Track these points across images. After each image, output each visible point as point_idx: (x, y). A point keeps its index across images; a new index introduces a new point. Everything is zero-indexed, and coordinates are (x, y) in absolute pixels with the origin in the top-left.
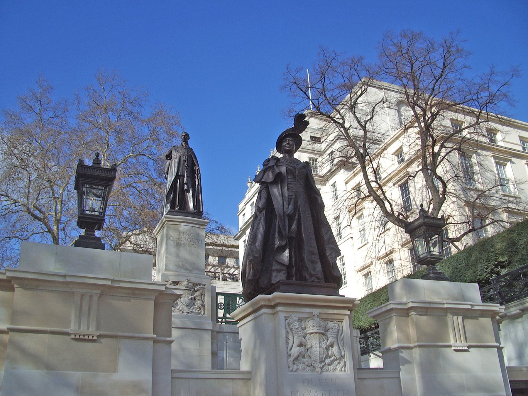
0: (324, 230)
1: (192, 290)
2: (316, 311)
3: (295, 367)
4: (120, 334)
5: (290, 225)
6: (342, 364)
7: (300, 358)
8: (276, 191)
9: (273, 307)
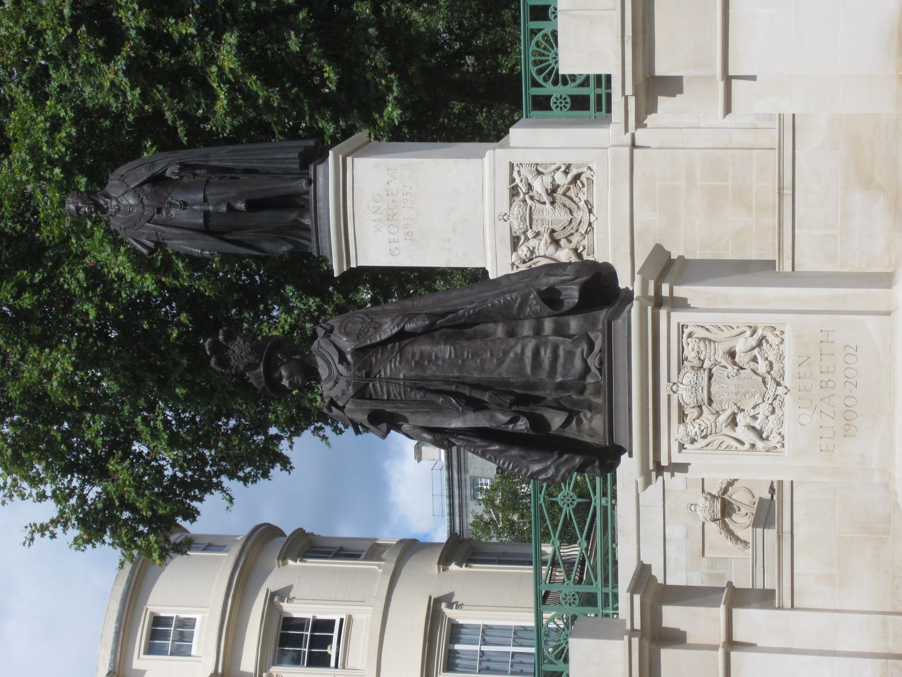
1: (529, 202)
3: (774, 440)
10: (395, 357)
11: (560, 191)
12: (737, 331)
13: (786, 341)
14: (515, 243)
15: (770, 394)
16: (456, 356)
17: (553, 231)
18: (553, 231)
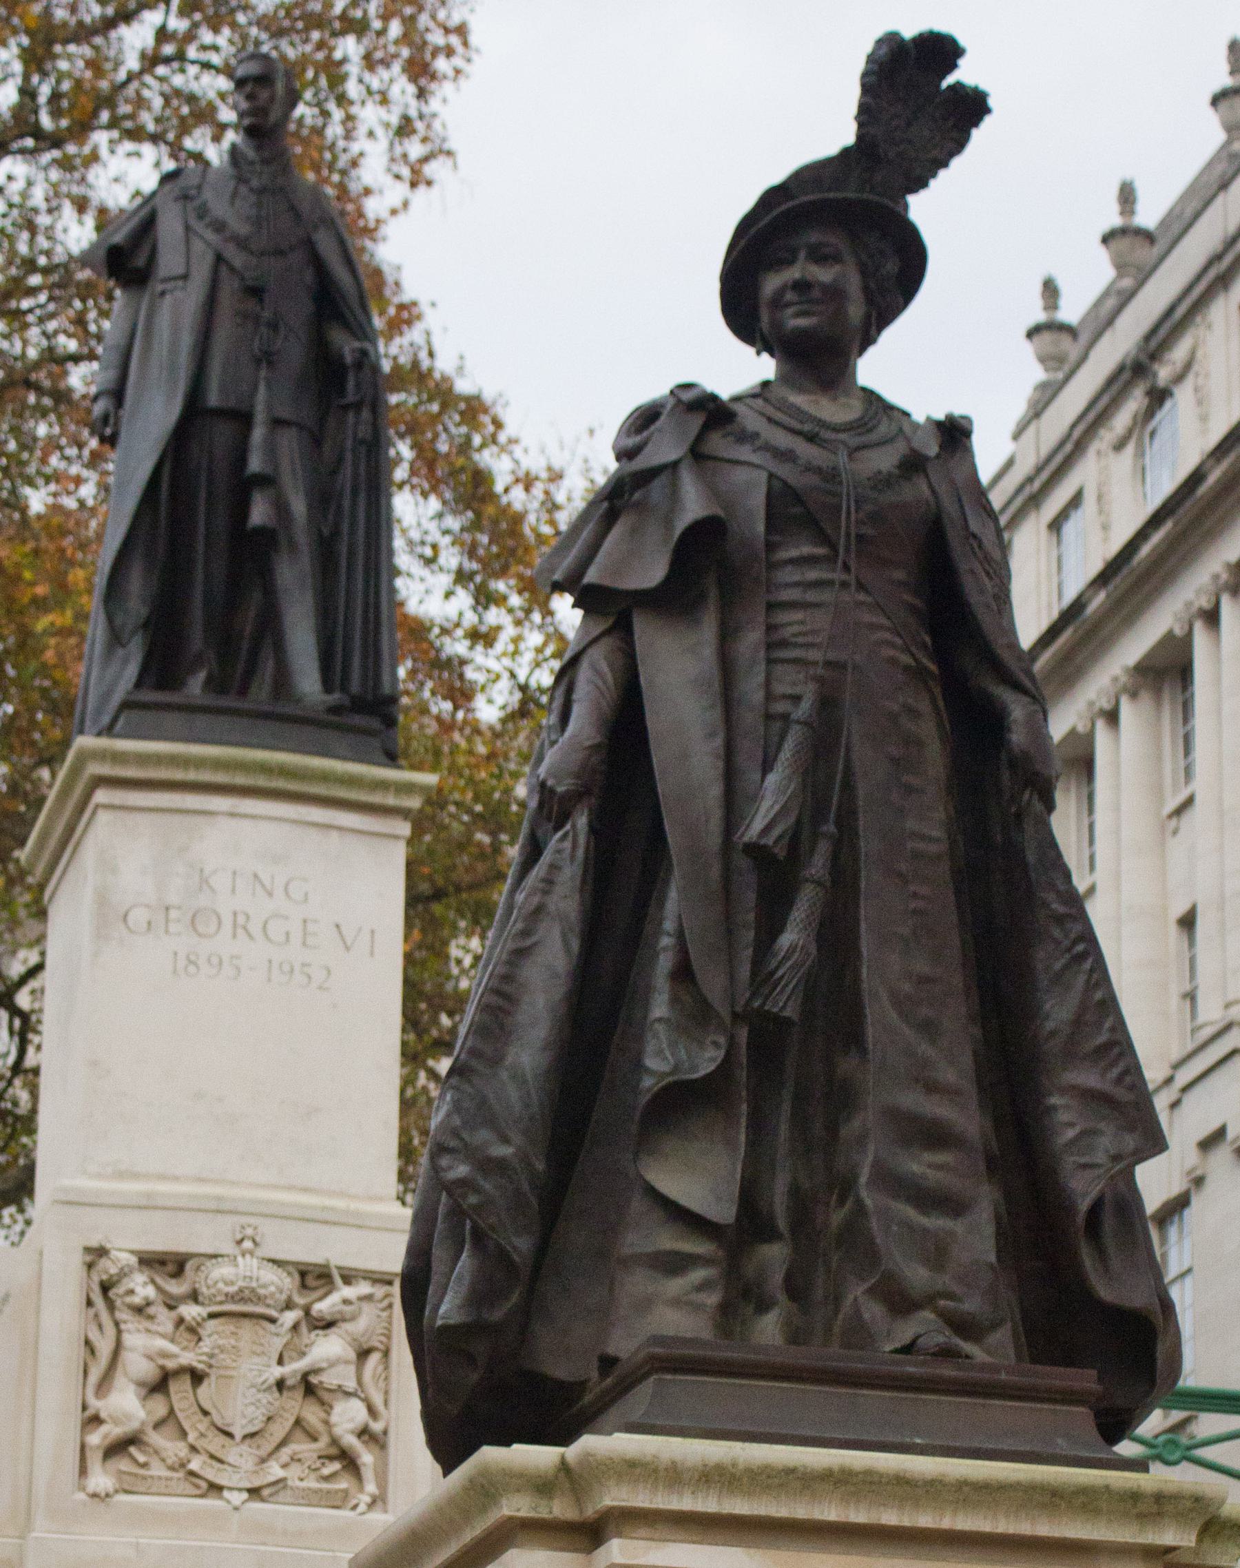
0: (1047, 959)
1: (290, 1317)
5: (770, 926)
8: (677, 666)
9: (590, 1533)
10: (907, 650)
11: (312, 1415)
14: (169, 1264)
16: (917, 855)
17: (197, 1377)
18: (197, 1377)
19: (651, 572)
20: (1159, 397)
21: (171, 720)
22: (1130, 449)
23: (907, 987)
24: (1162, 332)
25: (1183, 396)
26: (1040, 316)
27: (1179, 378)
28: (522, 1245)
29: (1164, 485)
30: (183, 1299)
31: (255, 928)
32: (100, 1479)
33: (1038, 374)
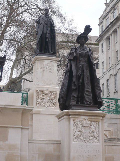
2: (87, 118)
3: (76, 140)
4: (8, 126)
5: (79, 80)
6: (97, 140)
7: (79, 136)
9: (69, 115)
12: (98, 133)
13: (96, 143)
15: (85, 139)
17: (44, 99)
18: (44, 99)
19: (72, 58)
20: (115, 10)
21: (42, 55)
22: (112, 14)
23: (87, 83)
24: (115, 5)
25: (117, 10)
26: (106, 2)
27: (116, 8)
28: (65, 98)
29: (115, 17)
30: (43, 94)
31: (47, 68)
32: (38, 106)
33: (105, 7)
